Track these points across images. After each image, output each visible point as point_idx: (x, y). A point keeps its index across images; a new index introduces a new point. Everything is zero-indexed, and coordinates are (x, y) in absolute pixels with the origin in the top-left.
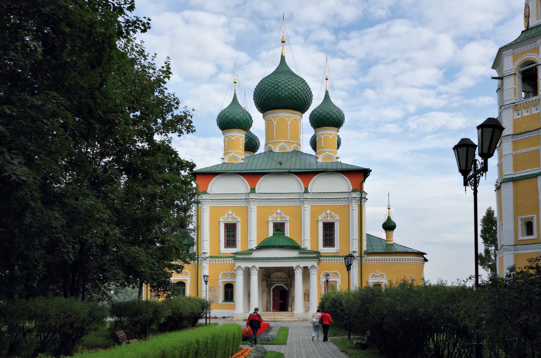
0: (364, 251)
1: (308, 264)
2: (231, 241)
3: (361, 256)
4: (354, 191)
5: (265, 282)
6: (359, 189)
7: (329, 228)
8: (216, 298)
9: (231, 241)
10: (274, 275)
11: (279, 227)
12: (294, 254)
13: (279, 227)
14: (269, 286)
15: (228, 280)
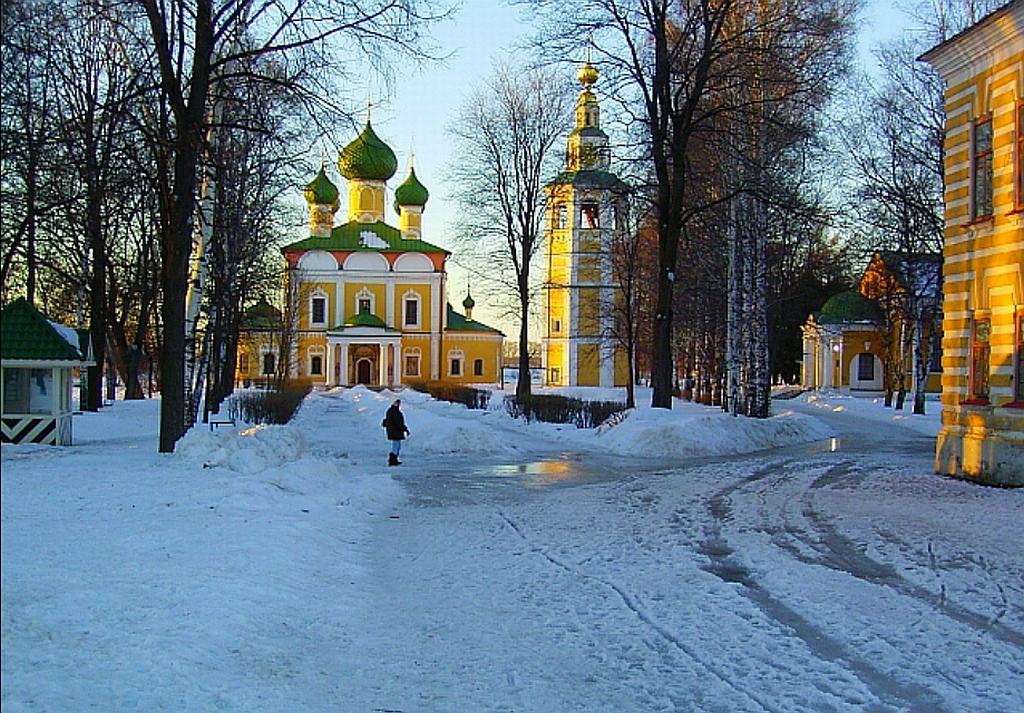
0: (445, 329)
1: (391, 341)
2: (319, 318)
3: (441, 333)
4: (435, 271)
5: (351, 357)
6: (440, 269)
7: (412, 305)
8: (305, 371)
9: (319, 318)
10: (359, 350)
11: (365, 306)
12: (382, 332)
13: (365, 306)
14: (355, 360)
15: (316, 354)
